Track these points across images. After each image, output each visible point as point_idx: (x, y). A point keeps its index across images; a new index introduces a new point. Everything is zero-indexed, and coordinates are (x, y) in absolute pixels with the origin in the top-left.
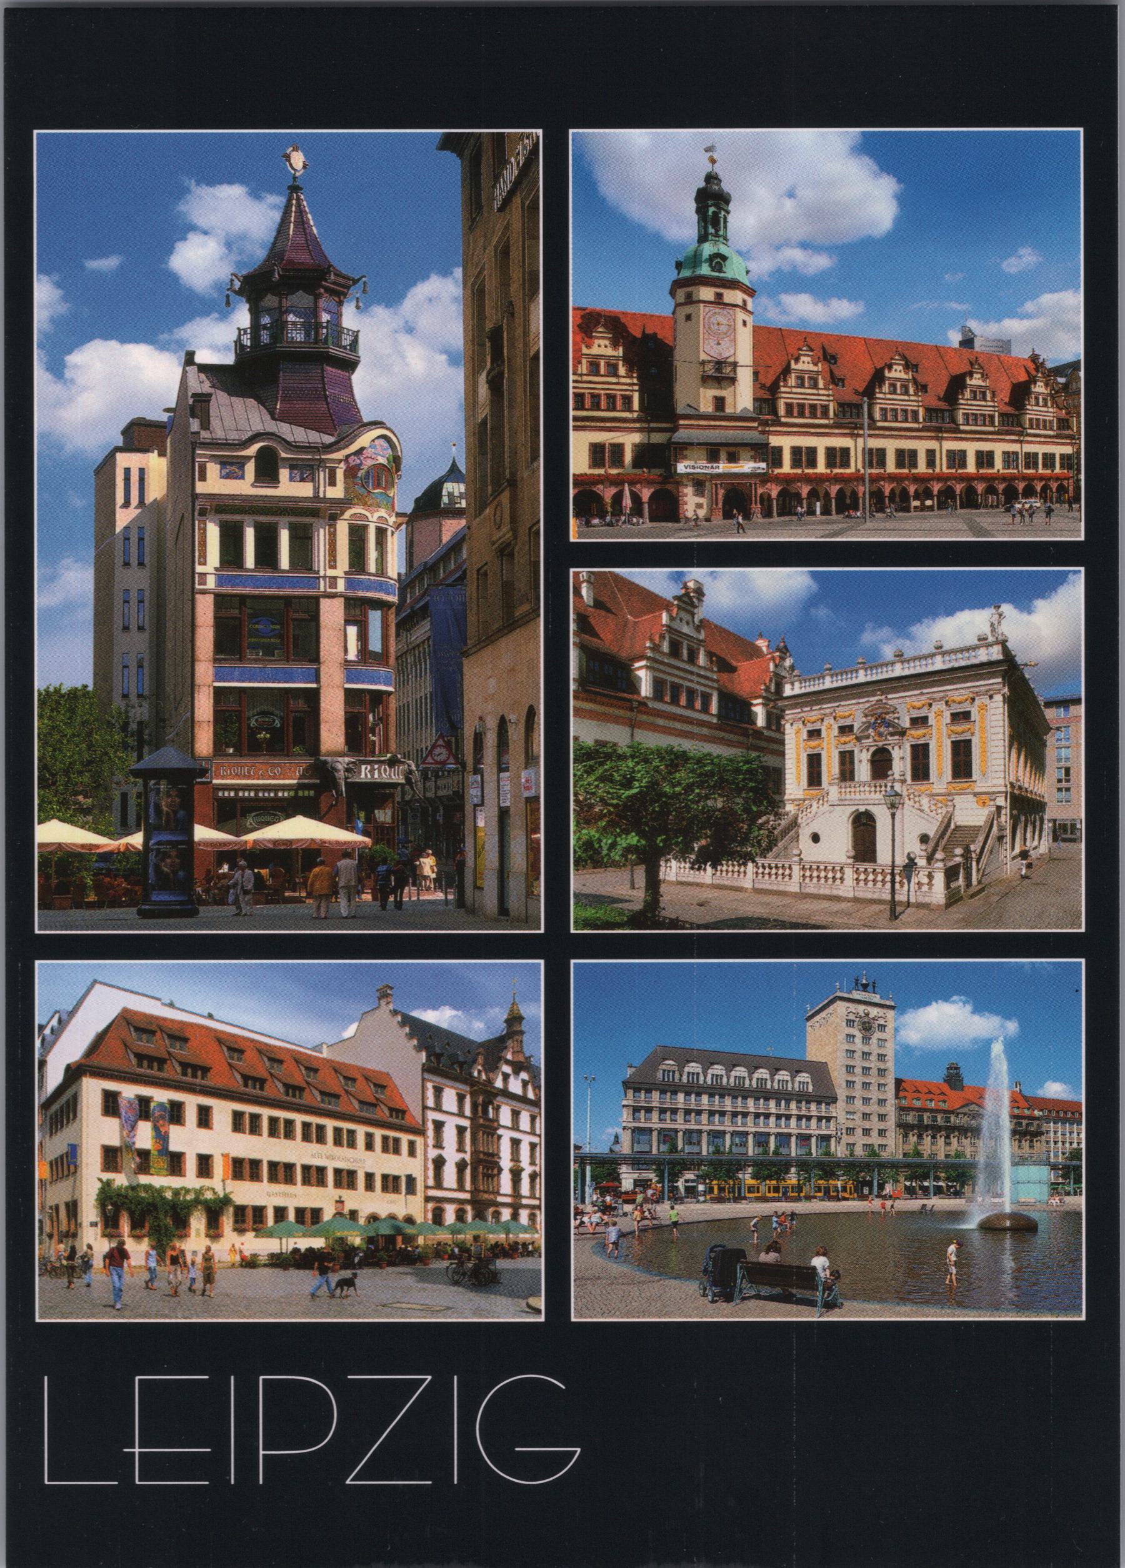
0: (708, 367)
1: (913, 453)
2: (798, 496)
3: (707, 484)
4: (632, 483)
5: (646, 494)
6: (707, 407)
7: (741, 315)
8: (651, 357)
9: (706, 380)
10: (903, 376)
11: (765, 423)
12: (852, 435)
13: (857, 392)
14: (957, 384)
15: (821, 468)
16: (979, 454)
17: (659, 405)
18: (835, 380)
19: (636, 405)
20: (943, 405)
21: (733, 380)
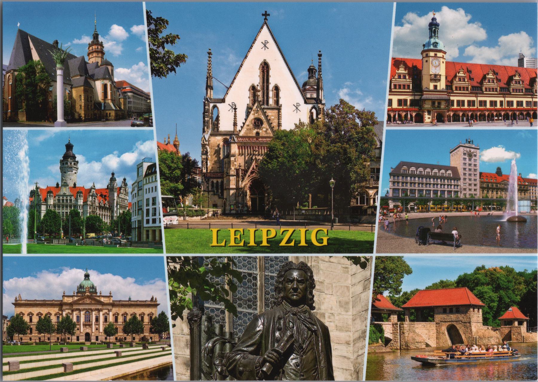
0: (433, 76)
1: (496, 102)
2: (459, 116)
5: (414, 114)
6: (432, 88)
7: (442, 60)
8: (416, 73)
9: (431, 80)
10: (492, 77)
11: (449, 93)
12: (476, 96)
13: (478, 83)
14: (510, 79)
15: (466, 106)
16: (518, 102)
17: (418, 87)
18: (471, 79)
19: (411, 88)
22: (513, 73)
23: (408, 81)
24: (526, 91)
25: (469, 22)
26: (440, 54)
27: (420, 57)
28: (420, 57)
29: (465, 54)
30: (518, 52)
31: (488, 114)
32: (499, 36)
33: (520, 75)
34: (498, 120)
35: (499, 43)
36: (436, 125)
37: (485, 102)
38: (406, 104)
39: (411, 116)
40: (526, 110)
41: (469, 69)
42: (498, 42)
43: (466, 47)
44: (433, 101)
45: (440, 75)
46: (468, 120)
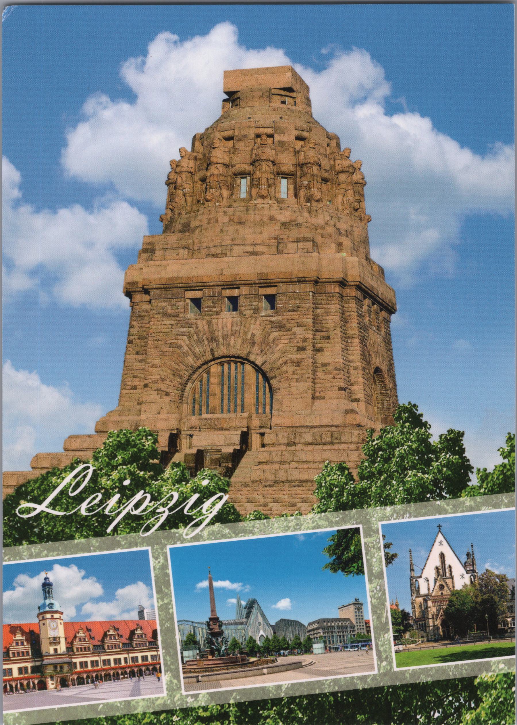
1: (120, 659)
2: (83, 678)
3: (55, 677)
4: (32, 679)
5: (36, 682)
6: (52, 652)
7: (59, 621)
8: (34, 638)
9: (51, 643)
11: (71, 655)
15: (90, 668)
16: (143, 657)
17: (37, 652)
18: (92, 638)
19: (30, 654)
20: (128, 641)
21: (59, 643)
22: (134, 627)
23: (26, 647)
24: (149, 645)
25: (84, 578)
26: (56, 616)
27: (36, 621)
28: (36, 621)
29: (83, 612)
30: (136, 604)
31: (114, 673)
32: (116, 590)
33: (141, 629)
34: (124, 678)
35: (117, 597)
36: (60, 690)
37: (109, 660)
38: (26, 672)
39: (34, 683)
40: (151, 665)
41: (89, 628)
42: (115, 596)
43: (83, 604)
44: (55, 666)
45: (59, 638)
46: (93, 682)
